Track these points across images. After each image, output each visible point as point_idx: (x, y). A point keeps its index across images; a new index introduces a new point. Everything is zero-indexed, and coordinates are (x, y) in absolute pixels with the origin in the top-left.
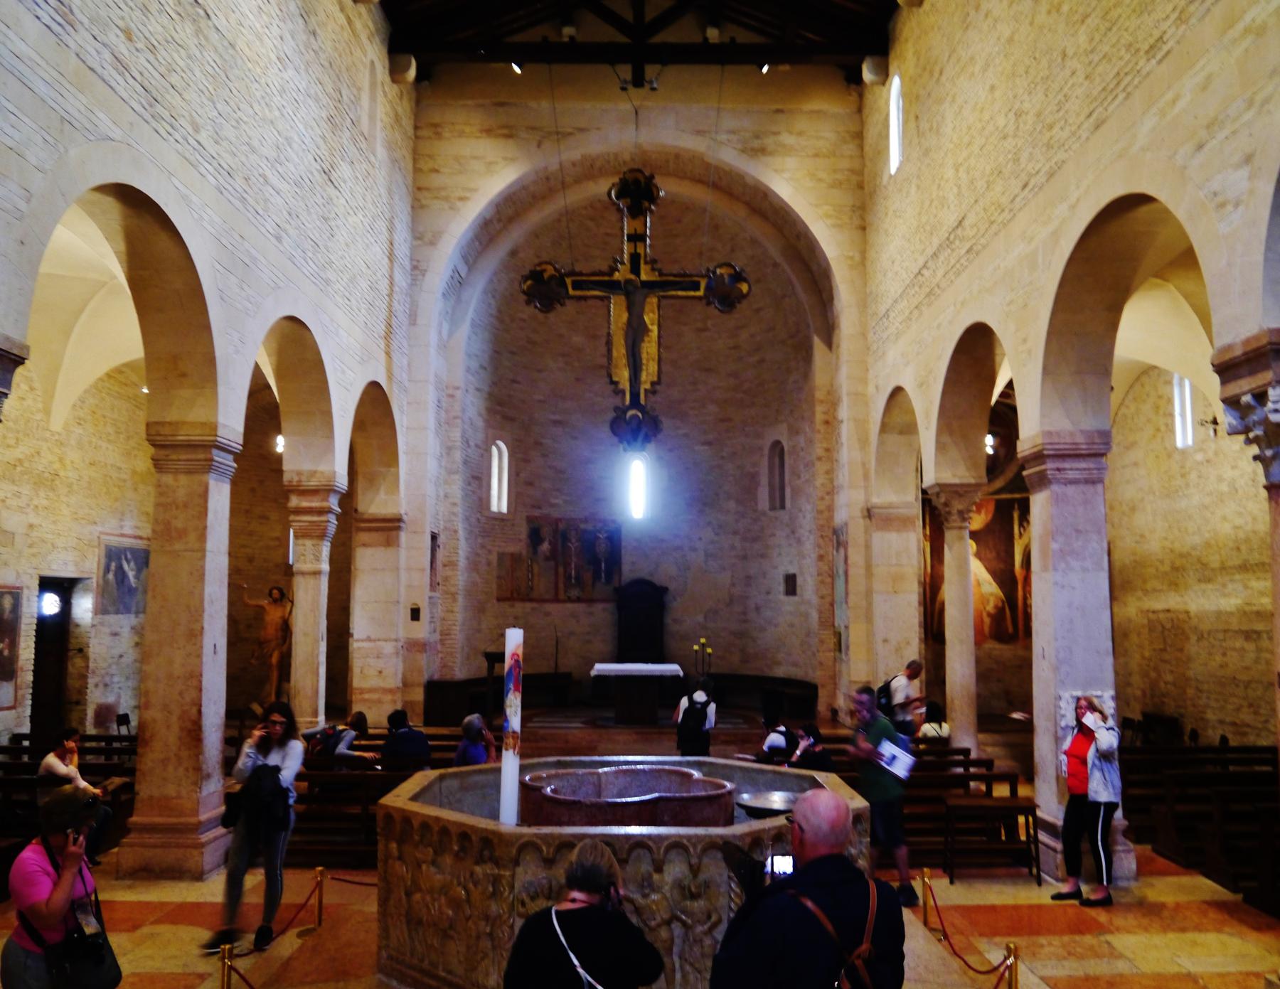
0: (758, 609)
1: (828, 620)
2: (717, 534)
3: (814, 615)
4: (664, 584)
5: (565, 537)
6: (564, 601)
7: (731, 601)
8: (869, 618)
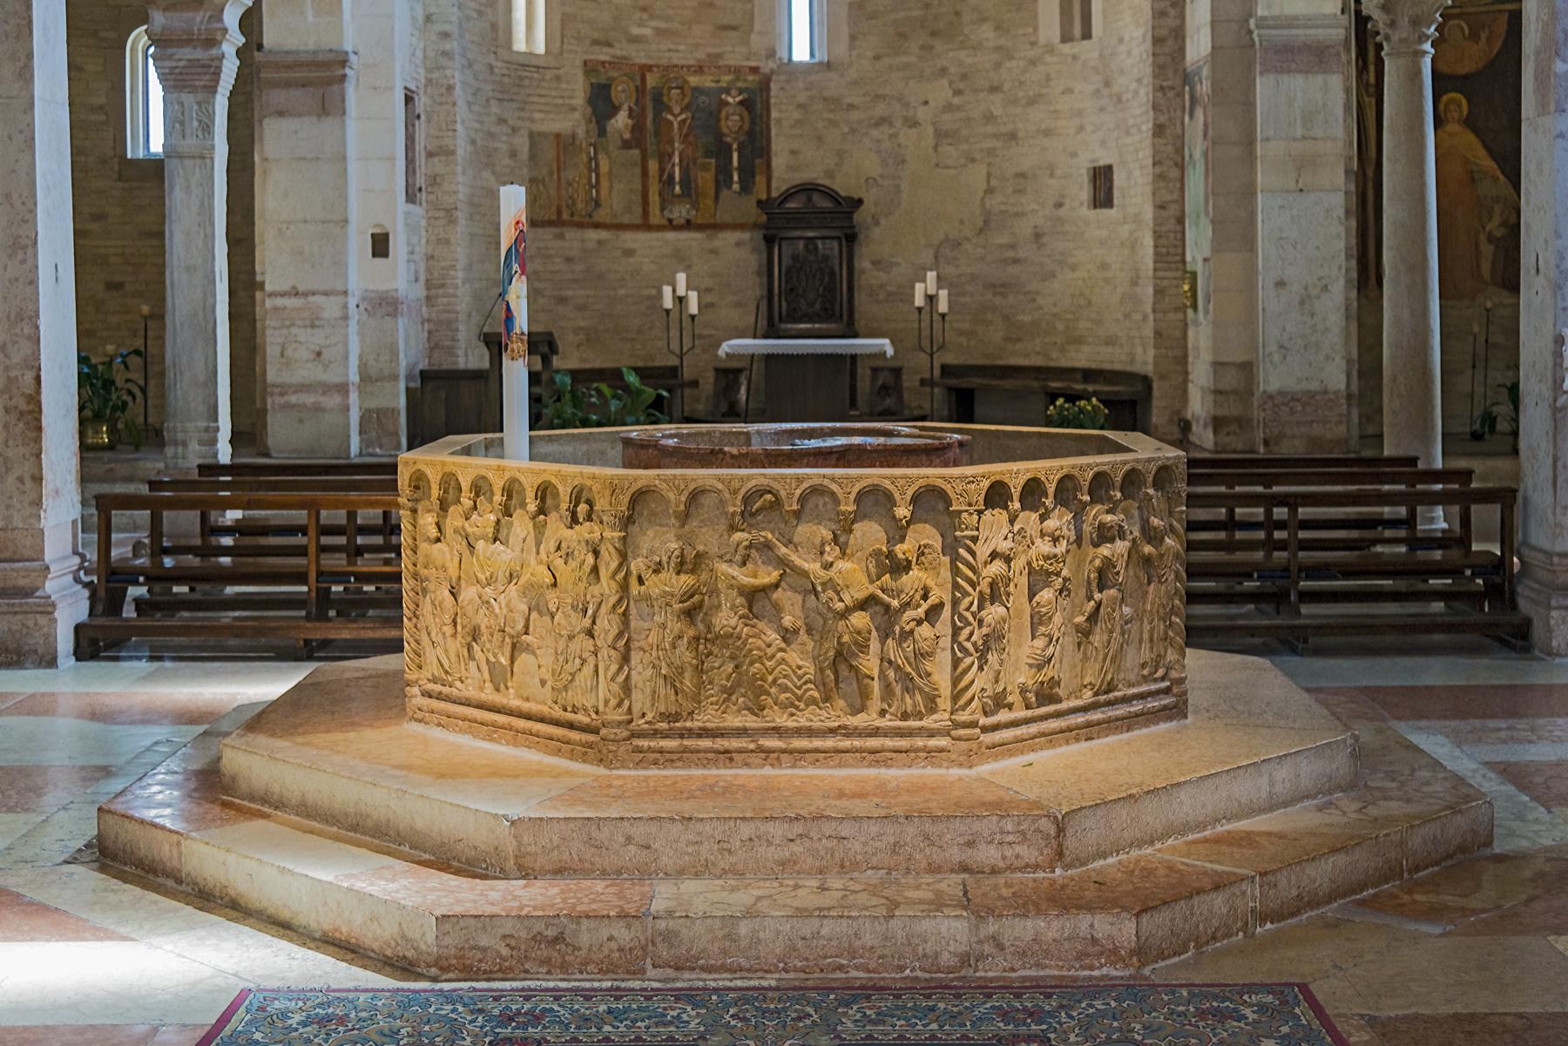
6: (660, 228)
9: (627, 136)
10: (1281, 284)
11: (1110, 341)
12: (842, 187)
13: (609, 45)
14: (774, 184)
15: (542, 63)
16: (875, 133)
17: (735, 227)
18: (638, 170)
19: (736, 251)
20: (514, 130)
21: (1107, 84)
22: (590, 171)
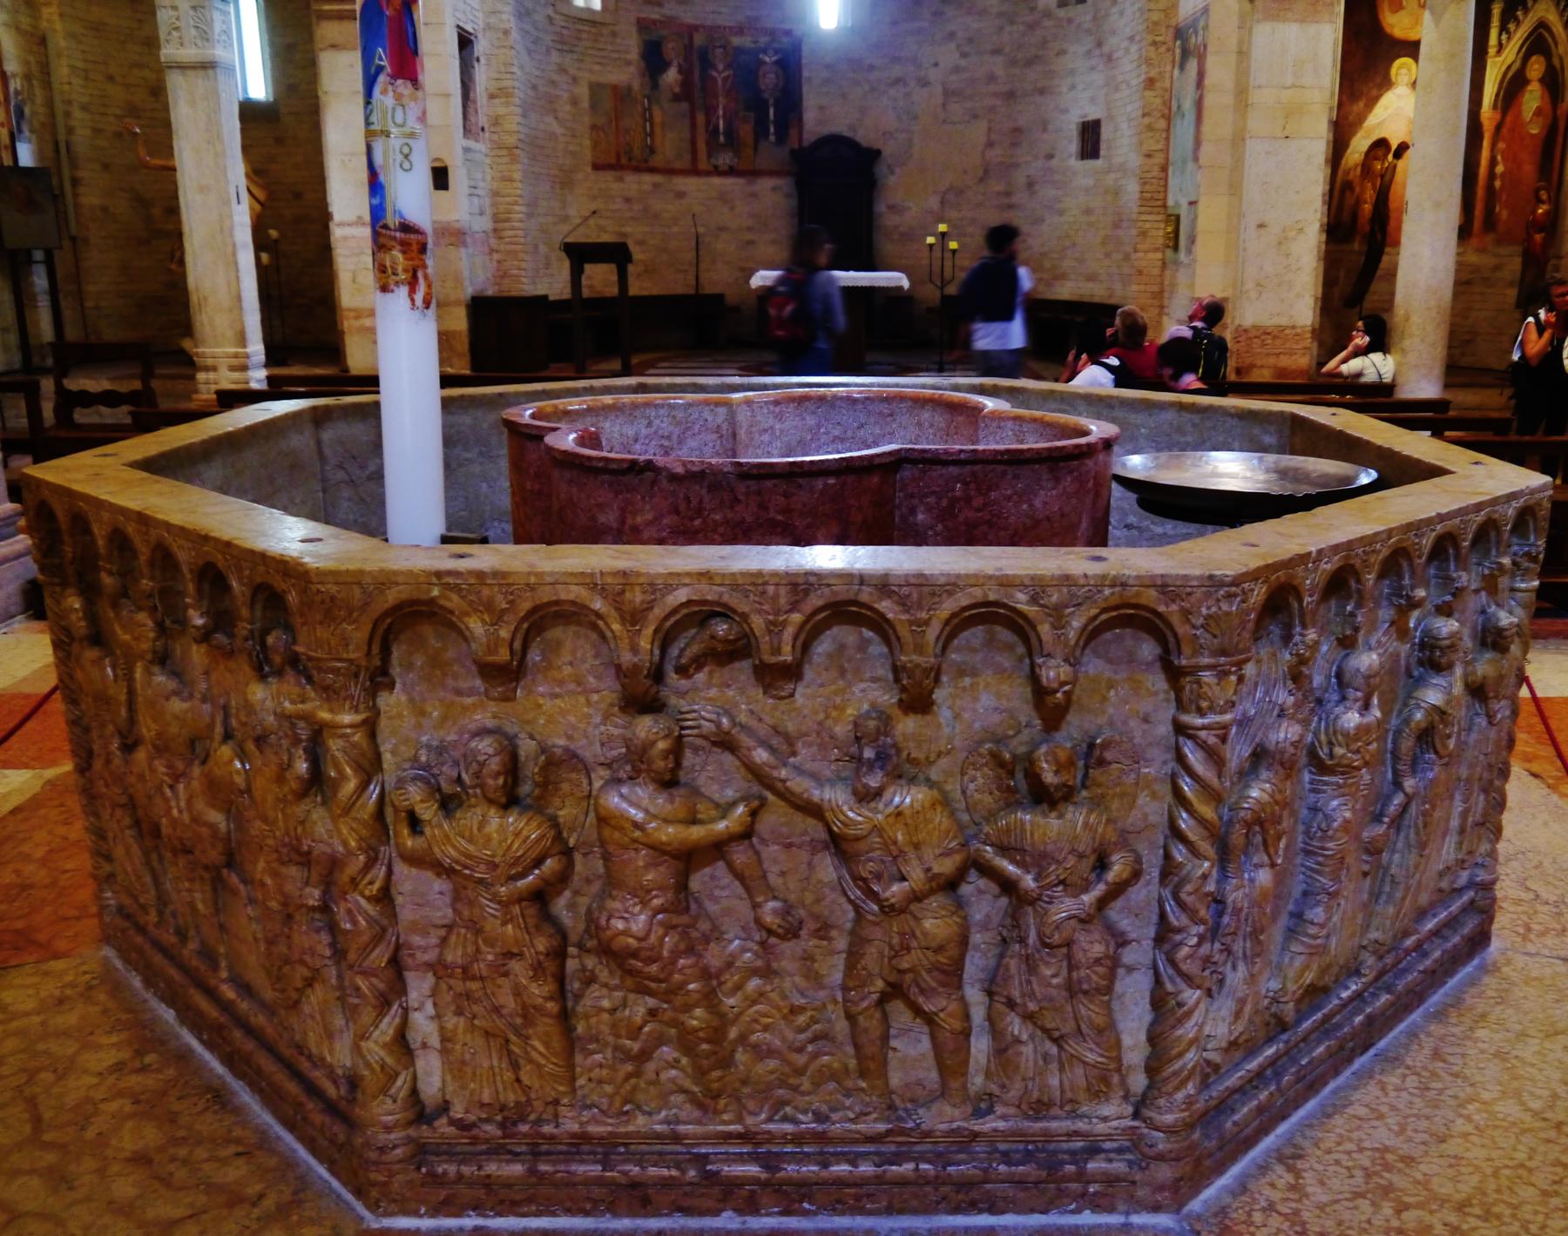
0: (1030, 185)
1: (1155, 196)
2: (964, 55)
3: (1132, 188)
4: (876, 146)
5: (706, 62)
6: (708, 174)
7: (986, 171)
8: (1235, 188)
9: (677, 90)
11: (1092, 278)
12: (864, 137)
14: (805, 136)
15: (598, 19)
16: (892, 92)
17: (771, 173)
19: (771, 197)
20: (575, 79)
21: (1099, 44)
22: (645, 120)
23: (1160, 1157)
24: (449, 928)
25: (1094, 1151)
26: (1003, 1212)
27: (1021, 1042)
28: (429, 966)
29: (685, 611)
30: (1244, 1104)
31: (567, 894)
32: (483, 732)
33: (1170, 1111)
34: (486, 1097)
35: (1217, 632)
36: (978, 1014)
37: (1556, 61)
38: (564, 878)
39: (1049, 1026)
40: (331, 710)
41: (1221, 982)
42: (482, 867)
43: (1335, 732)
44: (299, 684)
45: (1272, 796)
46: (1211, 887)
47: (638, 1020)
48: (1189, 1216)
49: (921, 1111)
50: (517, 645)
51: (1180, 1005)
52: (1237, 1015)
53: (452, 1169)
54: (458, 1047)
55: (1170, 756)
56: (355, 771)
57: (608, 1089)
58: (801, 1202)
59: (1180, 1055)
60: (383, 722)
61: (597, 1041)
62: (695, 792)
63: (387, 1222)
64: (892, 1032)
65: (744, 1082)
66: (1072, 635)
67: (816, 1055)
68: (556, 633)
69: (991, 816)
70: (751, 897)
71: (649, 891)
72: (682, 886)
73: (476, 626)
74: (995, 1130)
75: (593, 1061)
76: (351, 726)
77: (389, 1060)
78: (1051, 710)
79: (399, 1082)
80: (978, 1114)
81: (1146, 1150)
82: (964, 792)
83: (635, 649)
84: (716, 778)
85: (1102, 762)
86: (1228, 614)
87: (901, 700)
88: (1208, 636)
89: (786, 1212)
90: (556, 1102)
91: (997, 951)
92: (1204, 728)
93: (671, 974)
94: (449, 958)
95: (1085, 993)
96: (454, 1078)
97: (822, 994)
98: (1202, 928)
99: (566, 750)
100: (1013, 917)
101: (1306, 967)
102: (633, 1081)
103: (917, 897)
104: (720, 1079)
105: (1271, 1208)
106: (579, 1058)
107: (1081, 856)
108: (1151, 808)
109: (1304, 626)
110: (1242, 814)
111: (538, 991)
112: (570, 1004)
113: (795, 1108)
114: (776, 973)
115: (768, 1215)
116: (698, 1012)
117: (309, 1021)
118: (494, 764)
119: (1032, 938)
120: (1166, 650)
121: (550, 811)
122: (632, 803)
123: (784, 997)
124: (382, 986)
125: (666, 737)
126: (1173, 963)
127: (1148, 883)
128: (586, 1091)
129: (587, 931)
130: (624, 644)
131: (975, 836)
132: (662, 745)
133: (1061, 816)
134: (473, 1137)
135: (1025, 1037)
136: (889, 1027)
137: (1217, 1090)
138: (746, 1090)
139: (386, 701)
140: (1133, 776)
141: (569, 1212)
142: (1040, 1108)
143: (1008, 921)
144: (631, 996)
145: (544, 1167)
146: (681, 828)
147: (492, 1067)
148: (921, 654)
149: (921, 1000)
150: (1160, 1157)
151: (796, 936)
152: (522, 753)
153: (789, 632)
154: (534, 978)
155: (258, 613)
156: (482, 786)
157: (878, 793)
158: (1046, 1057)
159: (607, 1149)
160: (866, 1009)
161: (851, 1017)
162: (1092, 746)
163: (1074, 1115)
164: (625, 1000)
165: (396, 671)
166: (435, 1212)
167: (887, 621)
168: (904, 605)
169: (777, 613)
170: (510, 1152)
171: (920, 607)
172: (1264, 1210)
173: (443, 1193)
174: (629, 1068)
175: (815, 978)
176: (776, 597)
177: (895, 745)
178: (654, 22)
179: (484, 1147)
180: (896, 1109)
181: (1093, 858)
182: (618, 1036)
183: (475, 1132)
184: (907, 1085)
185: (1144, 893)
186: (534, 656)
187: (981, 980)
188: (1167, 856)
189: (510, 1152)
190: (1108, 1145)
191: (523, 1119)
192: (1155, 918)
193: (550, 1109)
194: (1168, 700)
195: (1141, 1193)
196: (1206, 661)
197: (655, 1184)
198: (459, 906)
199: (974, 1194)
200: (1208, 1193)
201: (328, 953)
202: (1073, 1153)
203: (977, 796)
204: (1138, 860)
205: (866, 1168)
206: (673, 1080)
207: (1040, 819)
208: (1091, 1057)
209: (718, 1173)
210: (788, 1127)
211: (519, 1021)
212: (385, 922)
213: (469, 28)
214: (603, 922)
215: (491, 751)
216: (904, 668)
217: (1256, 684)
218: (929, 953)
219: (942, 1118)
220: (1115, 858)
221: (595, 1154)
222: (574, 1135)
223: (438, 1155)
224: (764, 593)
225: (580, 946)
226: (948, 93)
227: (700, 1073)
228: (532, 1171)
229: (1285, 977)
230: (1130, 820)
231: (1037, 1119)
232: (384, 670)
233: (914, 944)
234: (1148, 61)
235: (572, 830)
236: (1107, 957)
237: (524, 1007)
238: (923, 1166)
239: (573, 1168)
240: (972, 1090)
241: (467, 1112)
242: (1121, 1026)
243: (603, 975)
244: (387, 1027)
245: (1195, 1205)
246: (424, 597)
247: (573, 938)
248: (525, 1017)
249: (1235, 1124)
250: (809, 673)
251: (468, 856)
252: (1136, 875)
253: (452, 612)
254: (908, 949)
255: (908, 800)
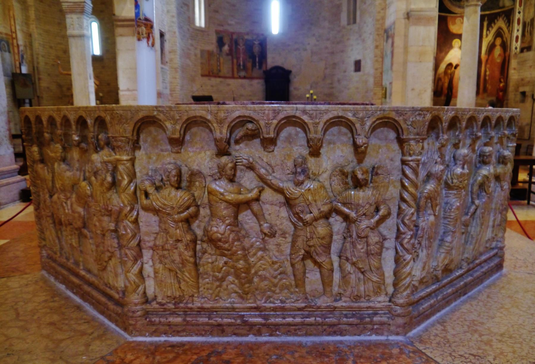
0: (339, 81)
1: (379, 83)
2: (318, 41)
3: (371, 80)
4: (290, 69)
5: (237, 43)
6: (237, 78)
7: (325, 77)
8: (404, 78)
9: (228, 52)
10: (413, 89)
12: (287, 67)
13: (222, 26)
18: (230, 62)
21: (360, 36)
22: (217, 61)
23: (399, 315)
24: (157, 234)
25: (376, 314)
26: (345, 335)
27: (351, 273)
28: (151, 248)
29: (238, 120)
30: (425, 303)
31: (197, 221)
32: (170, 163)
33: (402, 298)
34: (169, 294)
35: (415, 127)
36: (336, 265)
37: (505, 39)
38: (196, 215)
39: (361, 266)
40: (120, 155)
41: (418, 256)
42: (169, 209)
43: (453, 175)
44: (110, 152)
45: (434, 189)
46: (414, 218)
47: (221, 265)
48: (409, 337)
49: (316, 300)
50: (182, 132)
51: (405, 260)
52: (424, 268)
53: (157, 320)
54: (160, 275)
55: (400, 173)
56: (127, 177)
57: (211, 292)
58: (276, 331)
59: (405, 278)
60: (137, 161)
61: (207, 274)
62: (240, 185)
63: (135, 339)
64: (307, 271)
65: (257, 289)
66: (367, 128)
67: (281, 279)
68: (194, 130)
69: (340, 193)
70: (259, 223)
71: (225, 218)
72: (236, 217)
73: (168, 125)
74: (342, 306)
75: (205, 281)
76: (126, 160)
77: (137, 280)
78: (359, 152)
79: (140, 289)
80: (336, 301)
81: (394, 313)
82: (331, 185)
83: (221, 133)
84: (248, 180)
85: (377, 174)
86: (419, 121)
87: (310, 152)
88: (412, 128)
89: (271, 335)
90: (193, 296)
91: (342, 242)
92: (412, 161)
93: (232, 247)
94: (158, 243)
95: (373, 254)
96: (158, 287)
97: (283, 257)
98: (412, 233)
99: (198, 170)
100: (348, 229)
101: (445, 258)
102: (219, 289)
103: (316, 219)
104: (249, 287)
105: (436, 335)
106: (200, 281)
107: (371, 205)
108: (394, 191)
109: (443, 133)
110: (424, 194)
111: (188, 254)
112: (198, 261)
113: (274, 299)
114: (267, 250)
115: (265, 336)
116: (241, 262)
117: (110, 273)
118: (174, 173)
119: (354, 235)
120: (398, 134)
121: (192, 192)
122: (221, 187)
123: (270, 258)
124: (135, 254)
125: (232, 162)
126: (402, 245)
127: (393, 218)
128: (203, 292)
129: (204, 235)
130: (218, 132)
131: (335, 200)
132: (230, 165)
133: (364, 191)
134: (164, 309)
135: (352, 272)
136: (306, 269)
137: (417, 296)
138: (257, 292)
139: (138, 154)
140: (388, 179)
141: (197, 335)
142: (357, 298)
143: (346, 231)
144: (219, 257)
145: (188, 319)
146: (236, 195)
147: (171, 283)
148: (316, 134)
149: (317, 258)
150: (399, 315)
151: (274, 236)
152: (183, 172)
153: (273, 126)
154: (186, 249)
155: (96, 129)
156: (169, 181)
157: (302, 183)
158: (359, 279)
159: (211, 312)
160: (298, 261)
161: (293, 265)
162: (374, 168)
163: (369, 301)
164: (216, 259)
165: (141, 143)
166: (152, 334)
167: (305, 123)
168: (311, 117)
169: (269, 120)
170: (177, 314)
171: (316, 118)
172: (434, 336)
173: (154, 328)
174: (218, 283)
175: (280, 251)
176: (268, 114)
177: (307, 168)
178: (221, 31)
179: (168, 312)
180: (308, 299)
181: (375, 206)
182: (214, 272)
183: (165, 306)
184: (312, 291)
185: (392, 221)
186: (187, 137)
187: (337, 253)
188: (400, 208)
189: (177, 314)
190: (380, 312)
191: (181, 302)
192: (395, 231)
193: (191, 299)
194: (399, 153)
195: (392, 328)
196: (412, 137)
197: (226, 325)
198: (161, 225)
199: (335, 328)
200: (415, 331)
201: (116, 246)
202: (369, 314)
203: (335, 186)
204: (390, 209)
205: (298, 320)
206: (232, 288)
207: (357, 193)
208: (375, 279)
209: (247, 321)
210: (272, 305)
211: (180, 265)
212: (136, 231)
213: (163, 30)
214: (209, 229)
215: (173, 168)
216: (311, 139)
217: (428, 151)
218: (320, 240)
219: (323, 302)
220: (382, 207)
221: (206, 315)
222: (199, 308)
223: (152, 315)
224: (264, 113)
225: (202, 241)
226: (312, 53)
227: (242, 285)
228: (184, 320)
229: (438, 261)
230: (387, 196)
231: (356, 303)
232: (137, 141)
233: (314, 236)
234: (376, 40)
235: (199, 199)
236: (380, 242)
237: (182, 260)
238: (317, 319)
239: (198, 319)
240: (334, 292)
241: (163, 299)
242: (384, 269)
243: (209, 250)
244: (136, 269)
245: (410, 334)
246: (151, 115)
247: (199, 238)
248: (183, 264)
249: (423, 308)
250: (279, 143)
251: (165, 205)
252: (389, 214)
253: (160, 120)
254: (313, 238)
255: (312, 186)
